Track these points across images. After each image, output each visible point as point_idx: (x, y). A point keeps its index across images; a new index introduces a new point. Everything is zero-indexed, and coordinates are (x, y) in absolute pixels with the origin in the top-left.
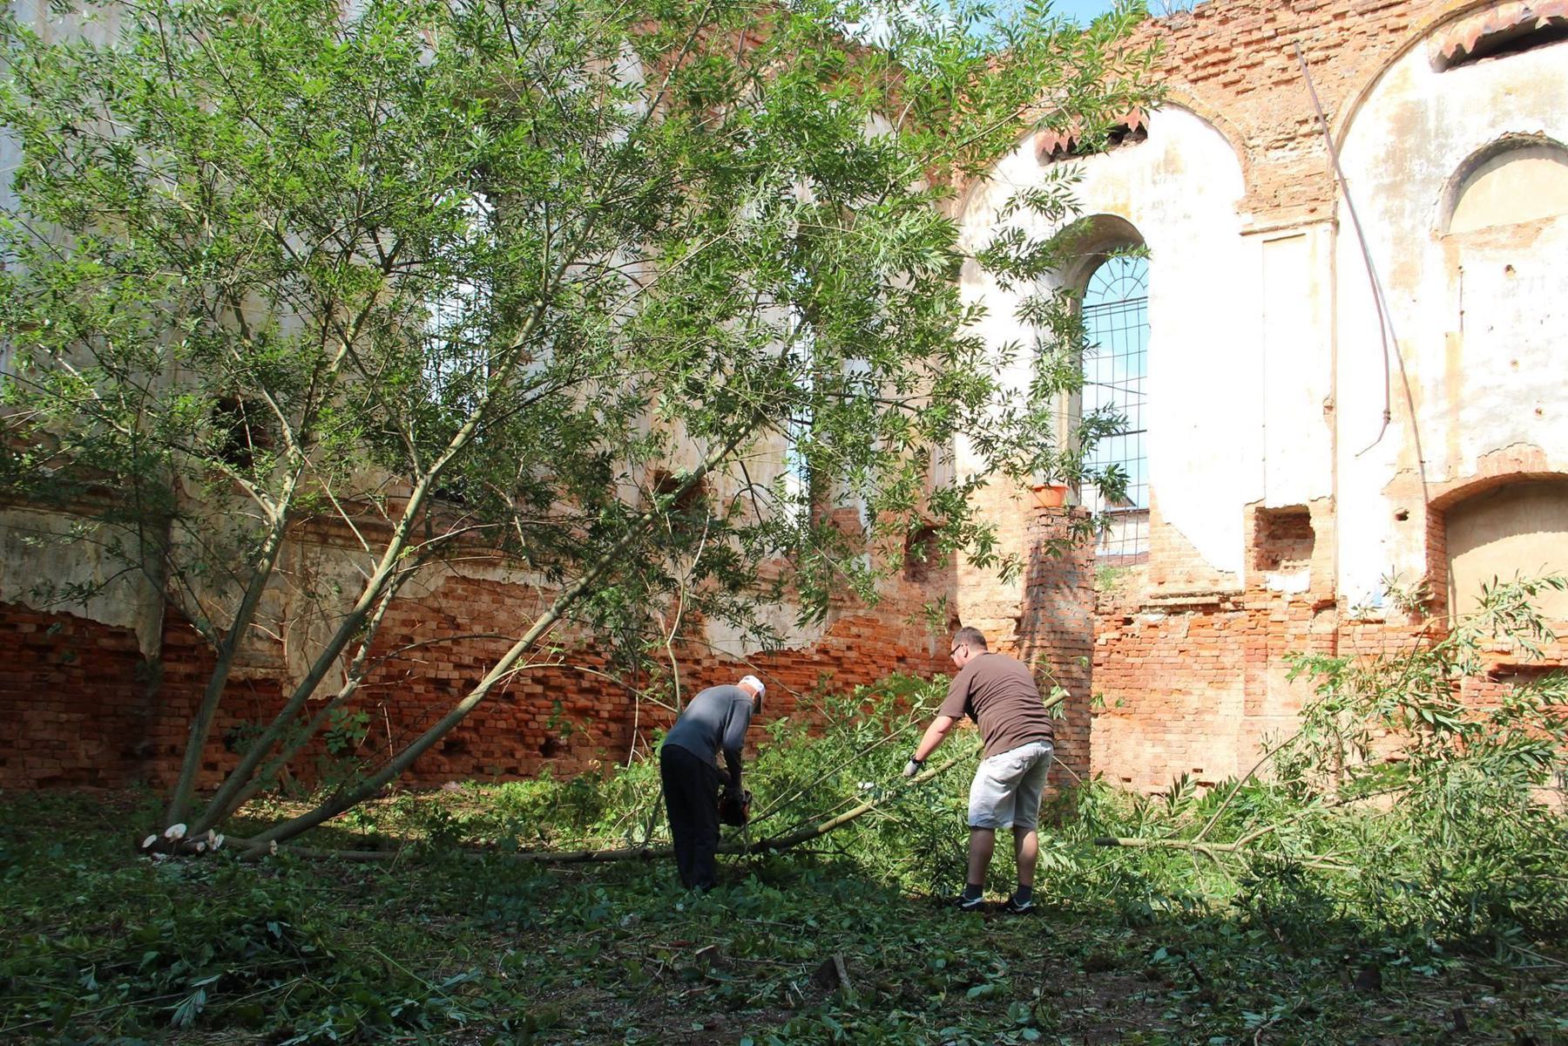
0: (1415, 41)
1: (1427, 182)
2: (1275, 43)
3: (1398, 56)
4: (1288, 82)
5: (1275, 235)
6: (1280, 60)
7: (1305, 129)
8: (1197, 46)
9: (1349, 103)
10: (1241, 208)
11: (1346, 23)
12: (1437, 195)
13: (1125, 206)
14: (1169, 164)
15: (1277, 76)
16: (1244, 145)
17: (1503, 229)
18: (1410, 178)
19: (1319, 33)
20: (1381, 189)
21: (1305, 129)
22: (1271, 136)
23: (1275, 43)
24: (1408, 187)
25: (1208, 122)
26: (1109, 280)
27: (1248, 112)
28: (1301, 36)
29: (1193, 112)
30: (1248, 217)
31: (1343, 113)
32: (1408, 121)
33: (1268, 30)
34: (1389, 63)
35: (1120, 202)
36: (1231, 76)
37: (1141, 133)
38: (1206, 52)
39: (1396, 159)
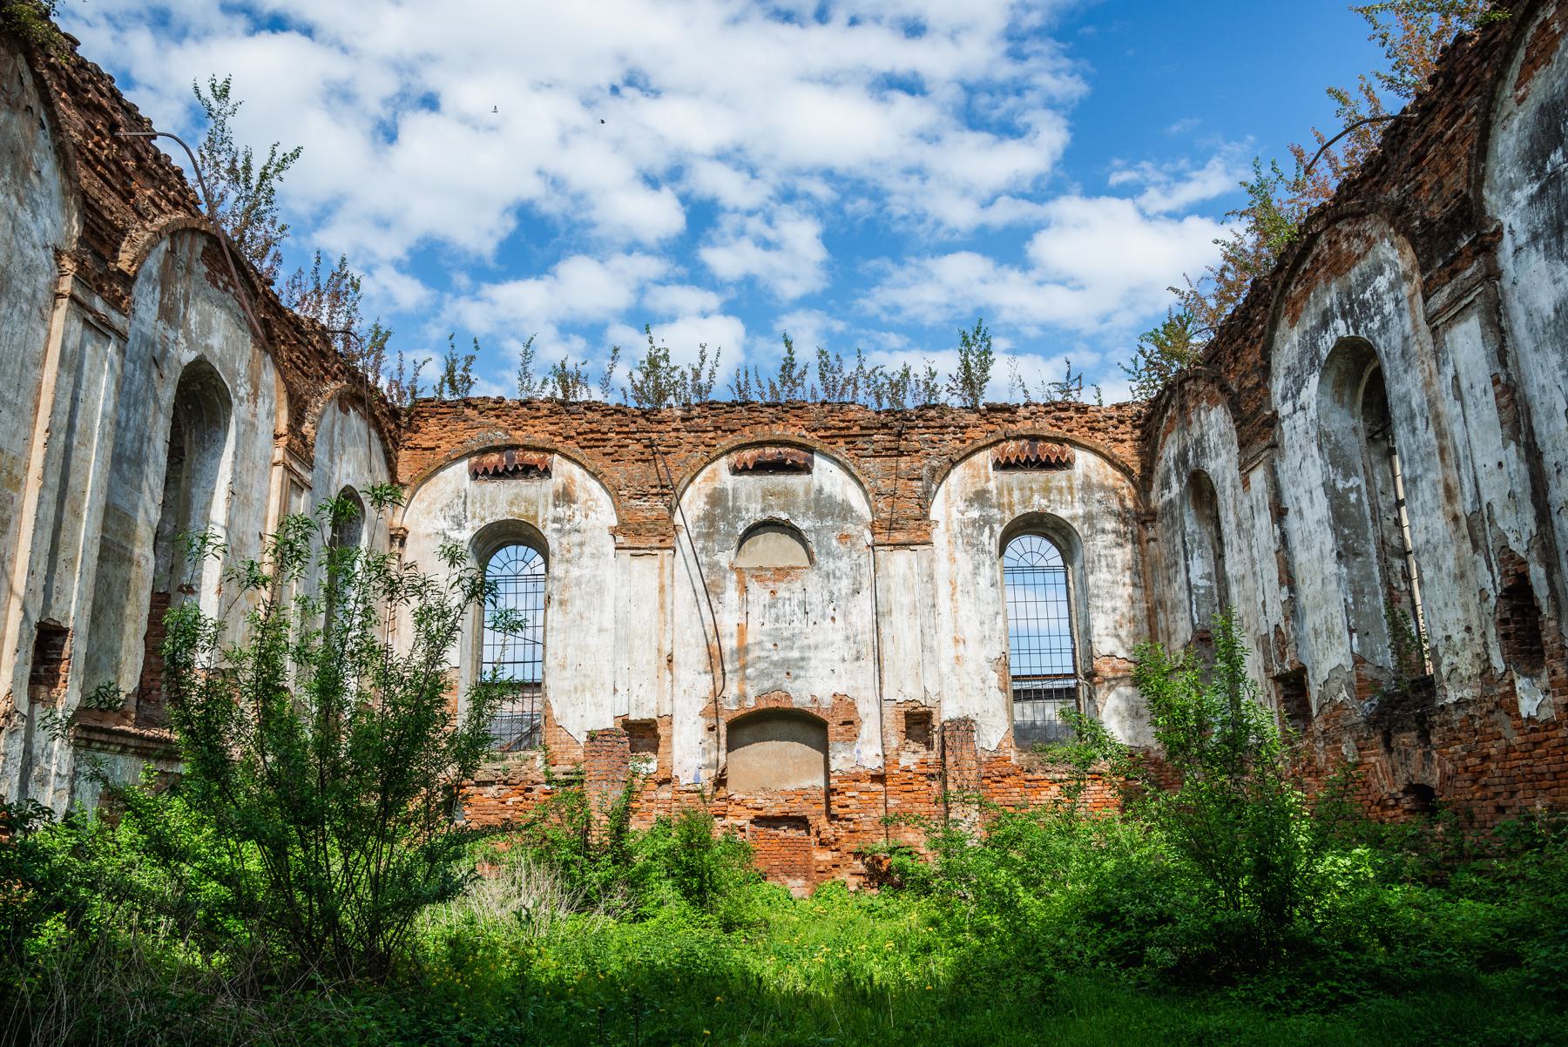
0: (721, 455)
1: (728, 534)
2: (637, 436)
3: (712, 461)
4: (644, 461)
5: (636, 551)
6: (638, 447)
7: (654, 491)
8: (586, 426)
9: (686, 480)
10: (614, 532)
11: (681, 435)
12: (734, 545)
13: (535, 517)
14: (565, 496)
15: (638, 456)
16: (614, 492)
17: (768, 569)
18: (718, 531)
19: (666, 437)
20: (699, 535)
21: (654, 491)
22: (633, 491)
23: (637, 436)
24: (716, 537)
25: (594, 475)
26: (513, 557)
27: (619, 473)
28: (654, 436)
29: (583, 467)
30: (620, 539)
31: (682, 486)
32: (716, 498)
33: (633, 427)
34: (707, 464)
35: (531, 513)
36: (608, 450)
37: (546, 472)
38: (592, 431)
39: (709, 519)
